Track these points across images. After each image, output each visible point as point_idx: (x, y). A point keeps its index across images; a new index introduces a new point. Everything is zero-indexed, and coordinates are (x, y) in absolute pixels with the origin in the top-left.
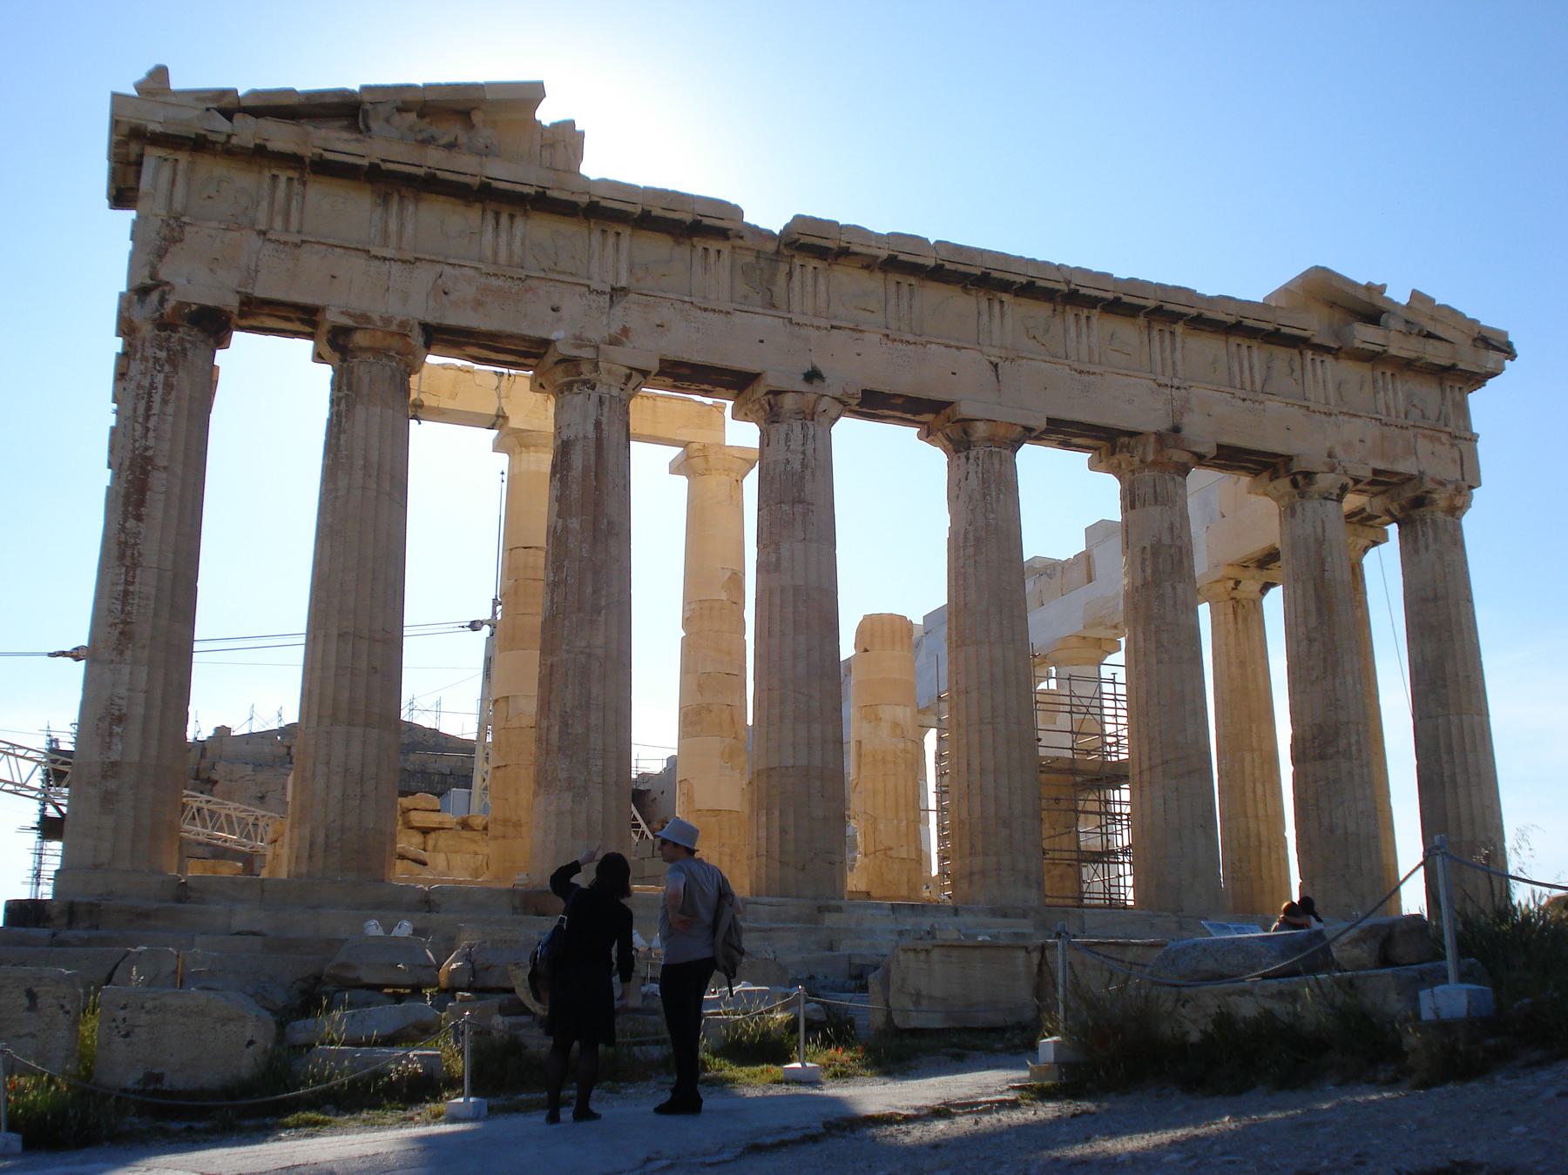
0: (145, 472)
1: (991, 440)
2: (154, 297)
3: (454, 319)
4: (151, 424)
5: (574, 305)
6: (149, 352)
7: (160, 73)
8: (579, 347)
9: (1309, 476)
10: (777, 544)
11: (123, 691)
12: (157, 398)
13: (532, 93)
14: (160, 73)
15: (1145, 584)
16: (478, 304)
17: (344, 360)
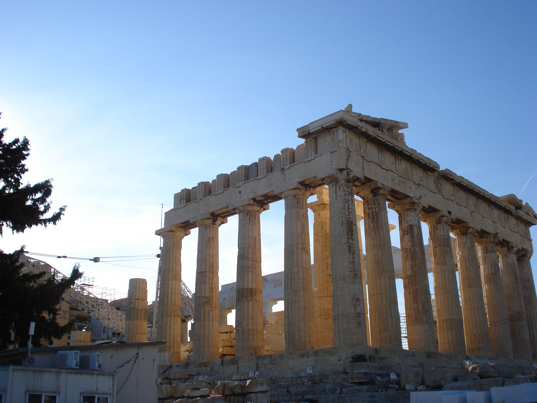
0: (352, 226)
1: (472, 233)
2: (345, 172)
3: (397, 188)
4: (350, 211)
5: (414, 187)
6: (345, 189)
7: (350, 106)
8: (416, 199)
9: (512, 247)
10: (445, 258)
11: (357, 292)
12: (350, 203)
13: (405, 126)
14: (350, 106)
15: (493, 273)
16: (399, 185)
17: (375, 196)
